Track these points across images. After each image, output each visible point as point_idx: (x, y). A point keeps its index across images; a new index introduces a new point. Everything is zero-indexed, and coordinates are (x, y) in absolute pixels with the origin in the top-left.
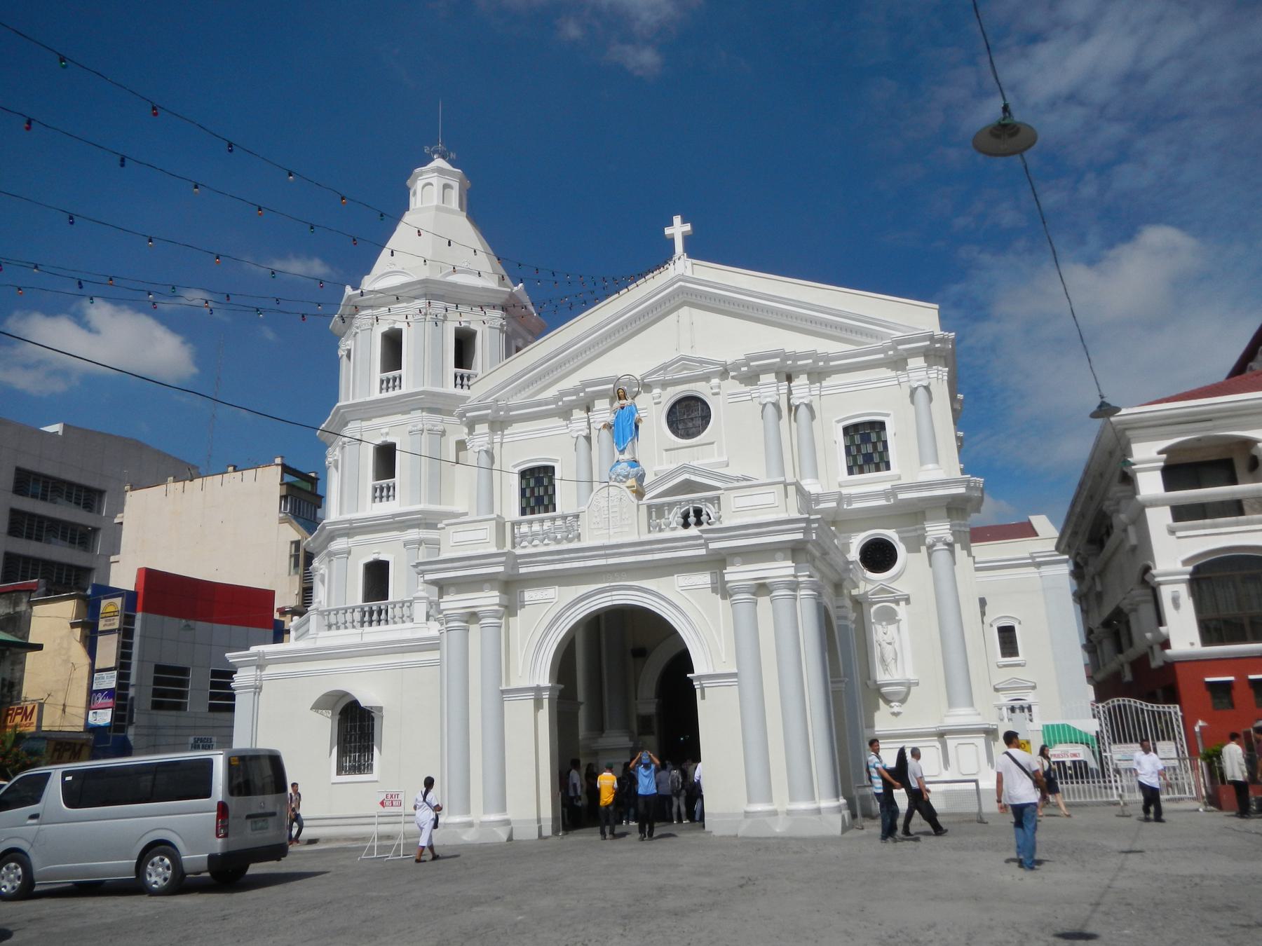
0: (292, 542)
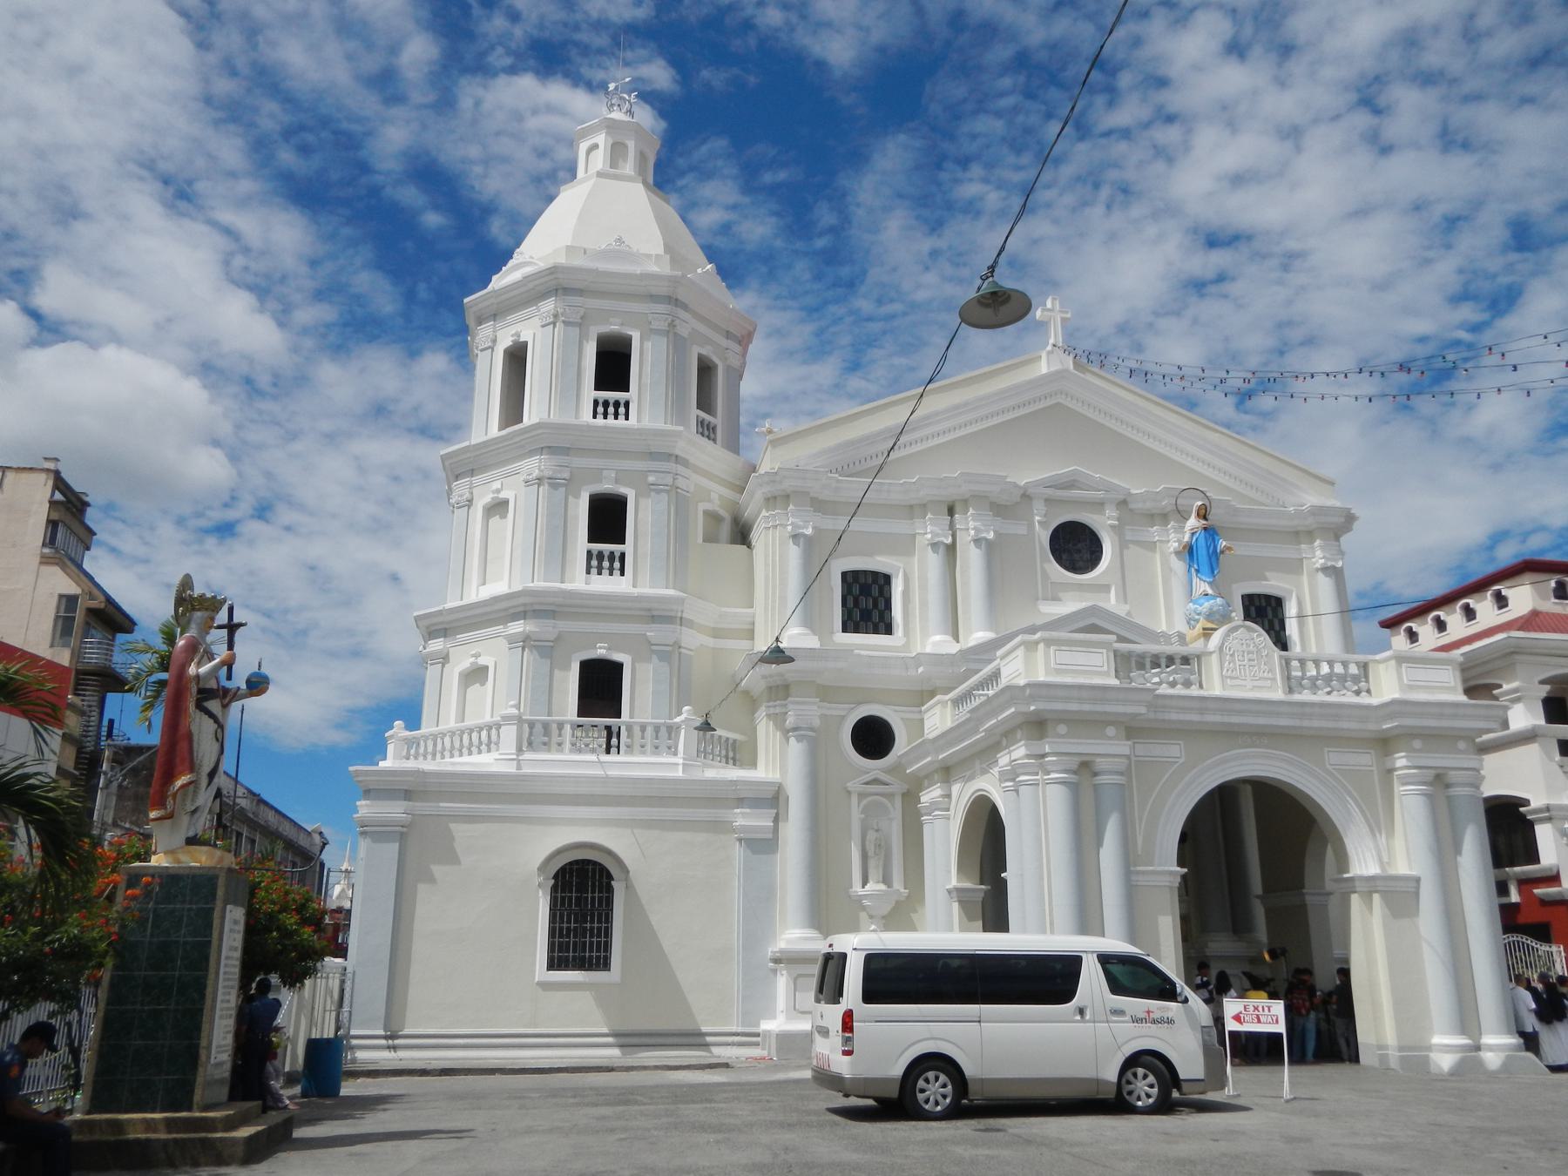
0: (61, 596)
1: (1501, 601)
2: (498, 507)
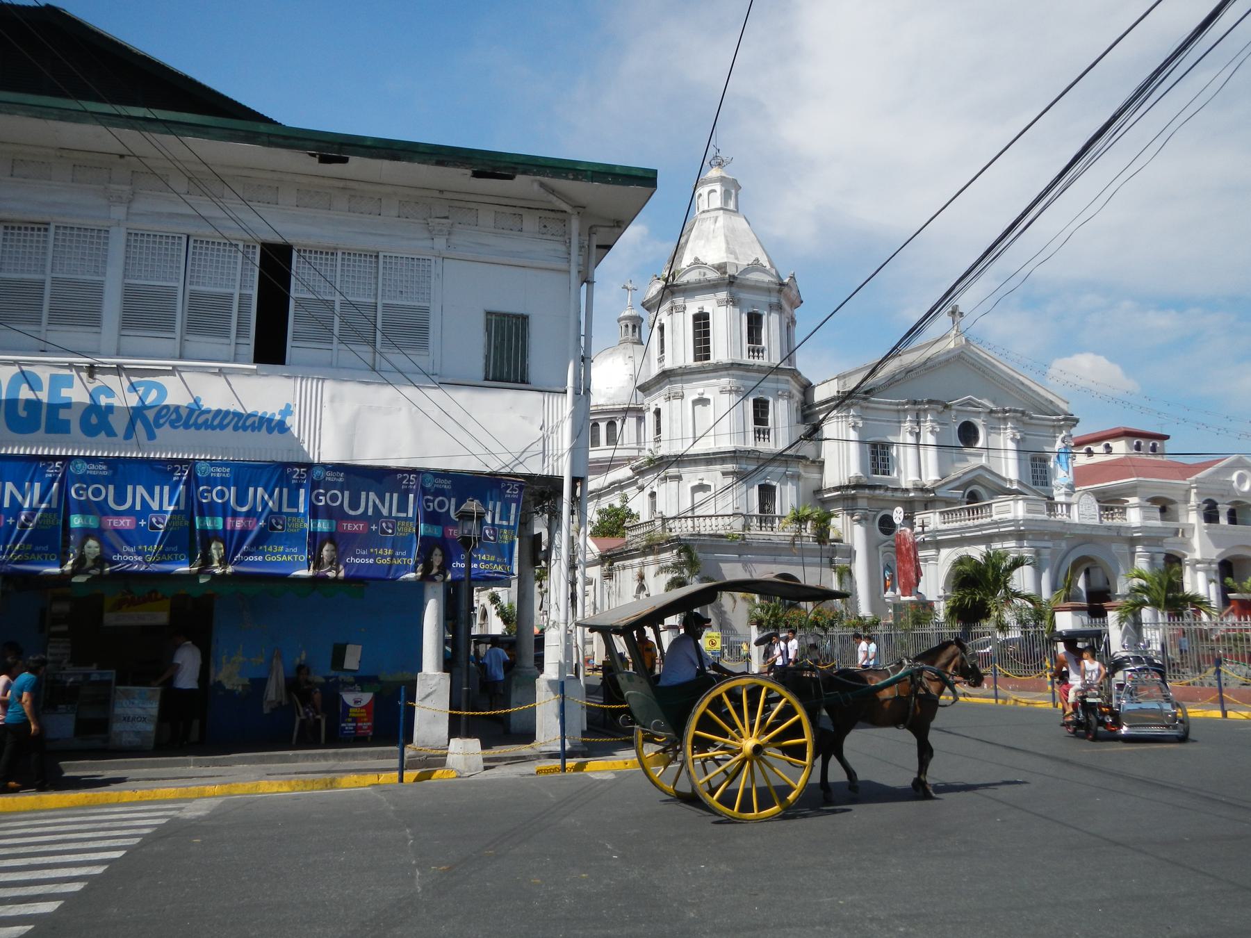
1: (1108, 449)
2: (702, 401)
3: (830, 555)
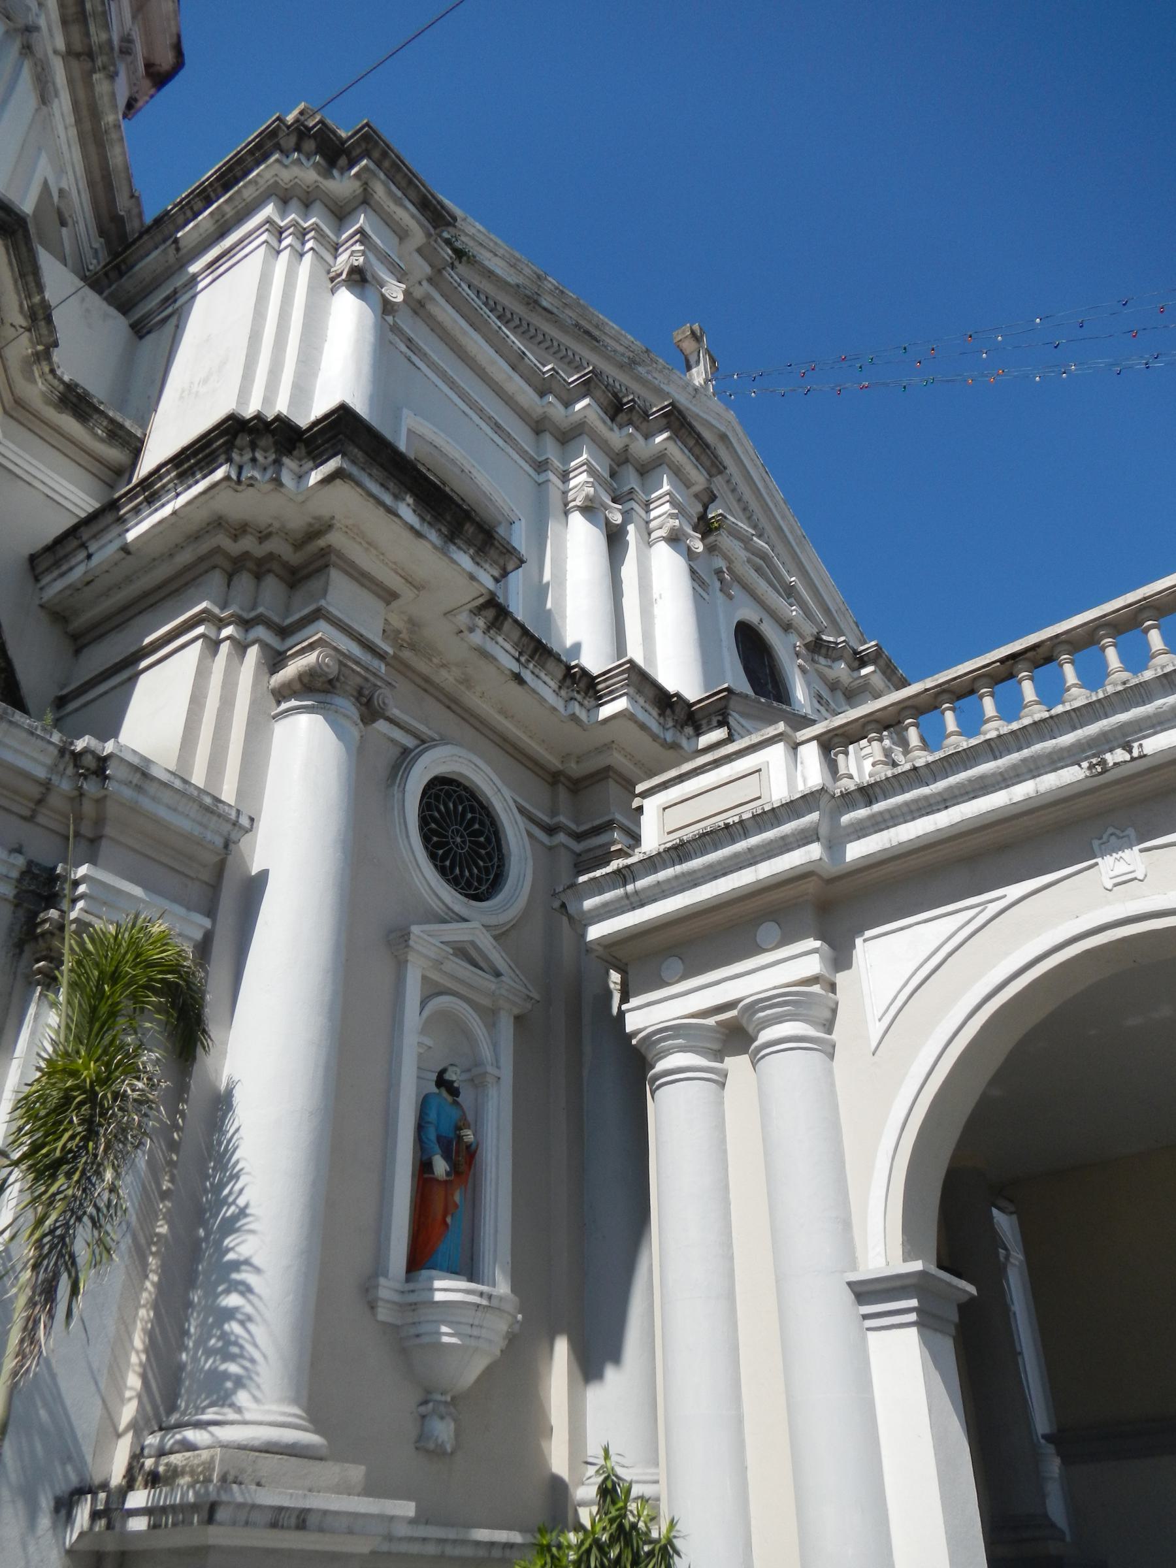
3: (42, 849)
